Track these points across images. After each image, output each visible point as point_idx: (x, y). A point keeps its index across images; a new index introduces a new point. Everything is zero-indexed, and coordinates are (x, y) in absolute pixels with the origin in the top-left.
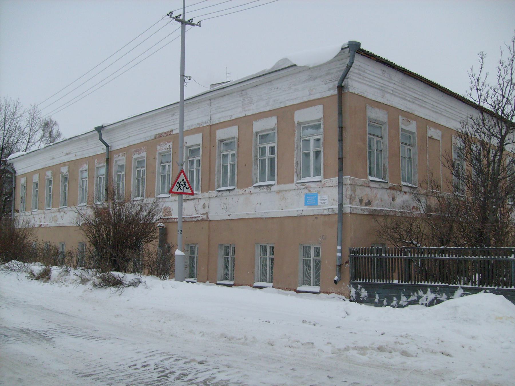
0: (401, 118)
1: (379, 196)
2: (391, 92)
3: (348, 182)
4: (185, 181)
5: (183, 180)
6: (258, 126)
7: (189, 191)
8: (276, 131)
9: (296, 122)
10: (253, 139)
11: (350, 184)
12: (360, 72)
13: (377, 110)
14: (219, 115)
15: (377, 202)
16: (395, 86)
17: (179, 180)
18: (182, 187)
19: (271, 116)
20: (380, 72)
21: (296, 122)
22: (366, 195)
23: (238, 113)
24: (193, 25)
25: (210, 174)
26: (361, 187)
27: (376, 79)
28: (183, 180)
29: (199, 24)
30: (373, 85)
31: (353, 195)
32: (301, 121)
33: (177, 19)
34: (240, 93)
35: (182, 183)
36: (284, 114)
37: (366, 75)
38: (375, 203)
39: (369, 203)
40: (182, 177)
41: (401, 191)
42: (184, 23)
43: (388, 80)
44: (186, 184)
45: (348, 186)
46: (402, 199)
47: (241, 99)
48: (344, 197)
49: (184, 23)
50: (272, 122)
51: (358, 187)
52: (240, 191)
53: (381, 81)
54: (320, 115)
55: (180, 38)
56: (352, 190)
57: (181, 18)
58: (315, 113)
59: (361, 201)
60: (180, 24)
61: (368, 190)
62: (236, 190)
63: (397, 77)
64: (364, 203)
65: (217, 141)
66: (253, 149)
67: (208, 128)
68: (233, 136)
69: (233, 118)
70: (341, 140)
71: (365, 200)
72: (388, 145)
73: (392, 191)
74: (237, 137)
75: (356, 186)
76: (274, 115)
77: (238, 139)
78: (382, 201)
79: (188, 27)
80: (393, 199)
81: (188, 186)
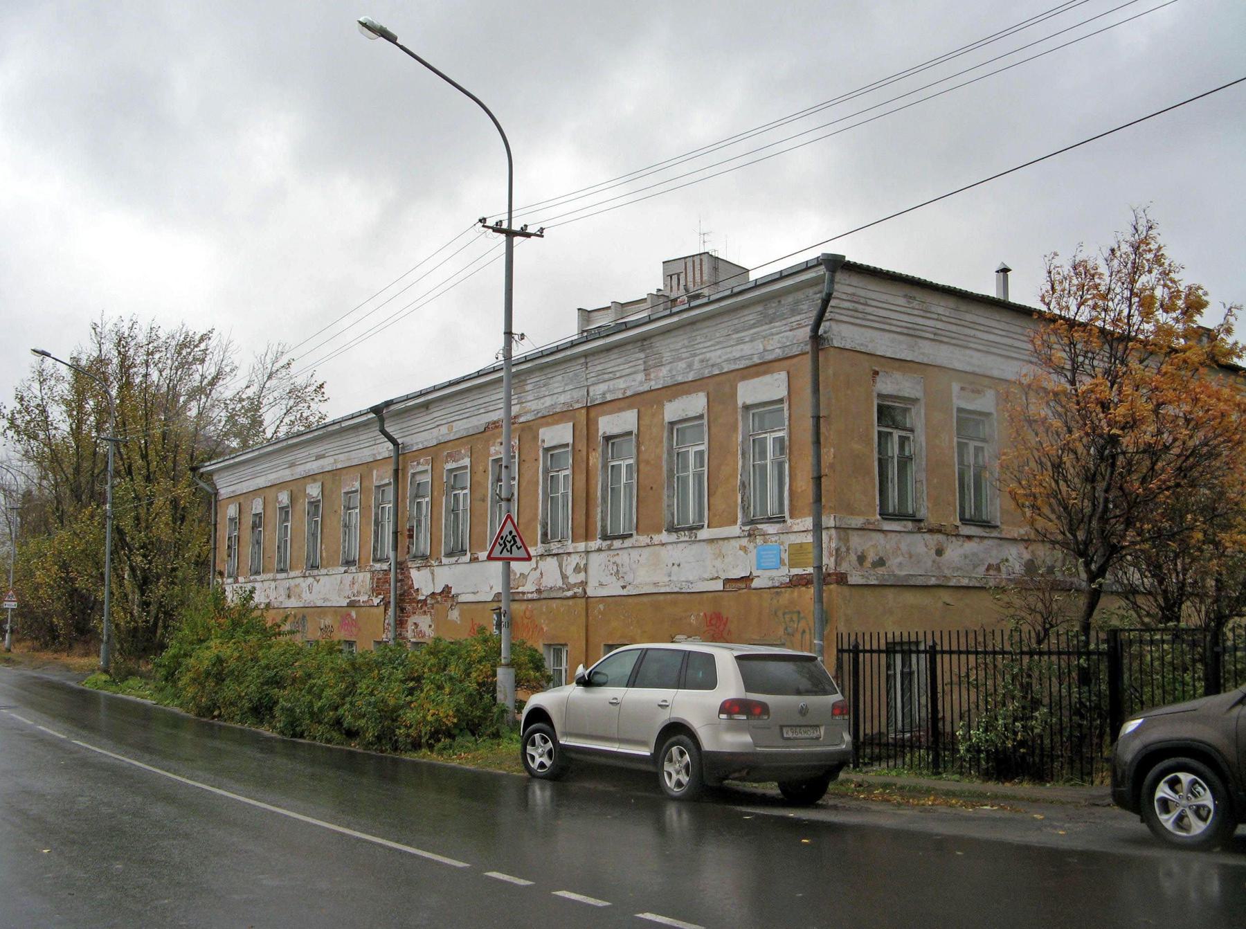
0: (955, 387)
1: (903, 547)
2: (932, 336)
3: (832, 523)
4: (514, 533)
5: (511, 533)
6: (673, 410)
7: (522, 553)
8: (705, 421)
9: (740, 403)
10: (665, 435)
11: (835, 528)
12: (857, 305)
13: (898, 375)
14: (602, 387)
15: (900, 559)
16: (939, 325)
17: (504, 534)
18: (509, 545)
19: (696, 391)
20: (901, 301)
21: (740, 403)
22: (875, 546)
23: (637, 383)
24: (529, 235)
25: (587, 503)
26: (860, 533)
27: (893, 315)
28: (511, 533)
29: (540, 234)
30: (887, 327)
31: (843, 549)
32: (749, 402)
33: (497, 229)
34: (639, 344)
35: (509, 538)
36: (719, 386)
37: (869, 310)
38: (893, 562)
39: (881, 562)
40: (509, 527)
41: (957, 535)
42: (510, 234)
43: (921, 313)
44: (517, 539)
45: (833, 532)
46: (960, 551)
47: (642, 355)
48: (825, 552)
49: (510, 234)
50: (696, 404)
51: (855, 533)
52: (644, 540)
53: (905, 318)
54: (782, 392)
55: (504, 258)
56: (840, 539)
57: (505, 226)
58: (772, 387)
59: (861, 559)
60: (503, 237)
61: (880, 536)
62: (635, 537)
63: (941, 307)
64: (868, 564)
65: (600, 439)
66: (665, 456)
67: (584, 411)
68: (628, 429)
69: (629, 393)
70: (817, 442)
71: (871, 557)
72: (924, 444)
73: (940, 537)
74: (635, 431)
75: (850, 532)
76: (702, 391)
77: (638, 436)
78: (911, 557)
79: (517, 240)
80: (939, 552)
81: (519, 544)
